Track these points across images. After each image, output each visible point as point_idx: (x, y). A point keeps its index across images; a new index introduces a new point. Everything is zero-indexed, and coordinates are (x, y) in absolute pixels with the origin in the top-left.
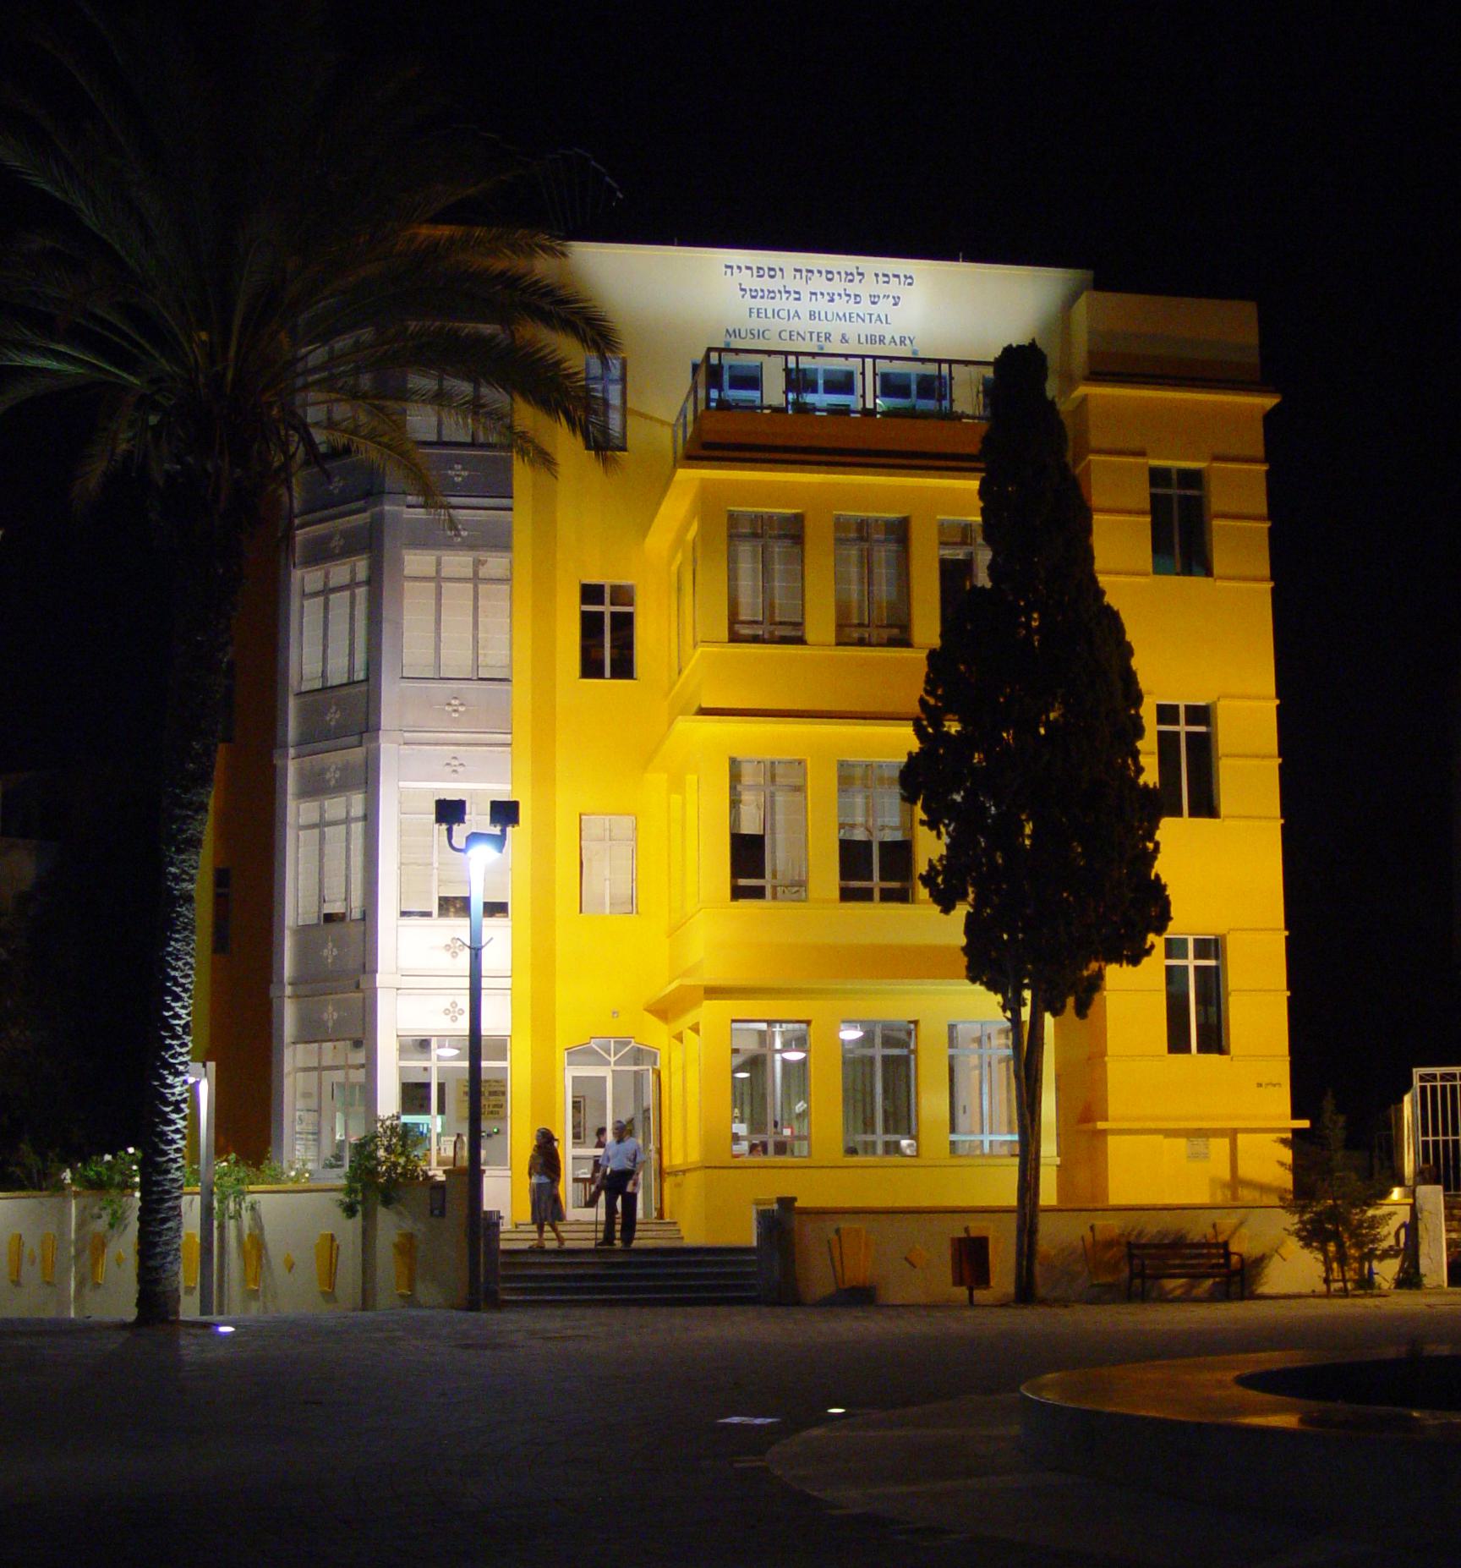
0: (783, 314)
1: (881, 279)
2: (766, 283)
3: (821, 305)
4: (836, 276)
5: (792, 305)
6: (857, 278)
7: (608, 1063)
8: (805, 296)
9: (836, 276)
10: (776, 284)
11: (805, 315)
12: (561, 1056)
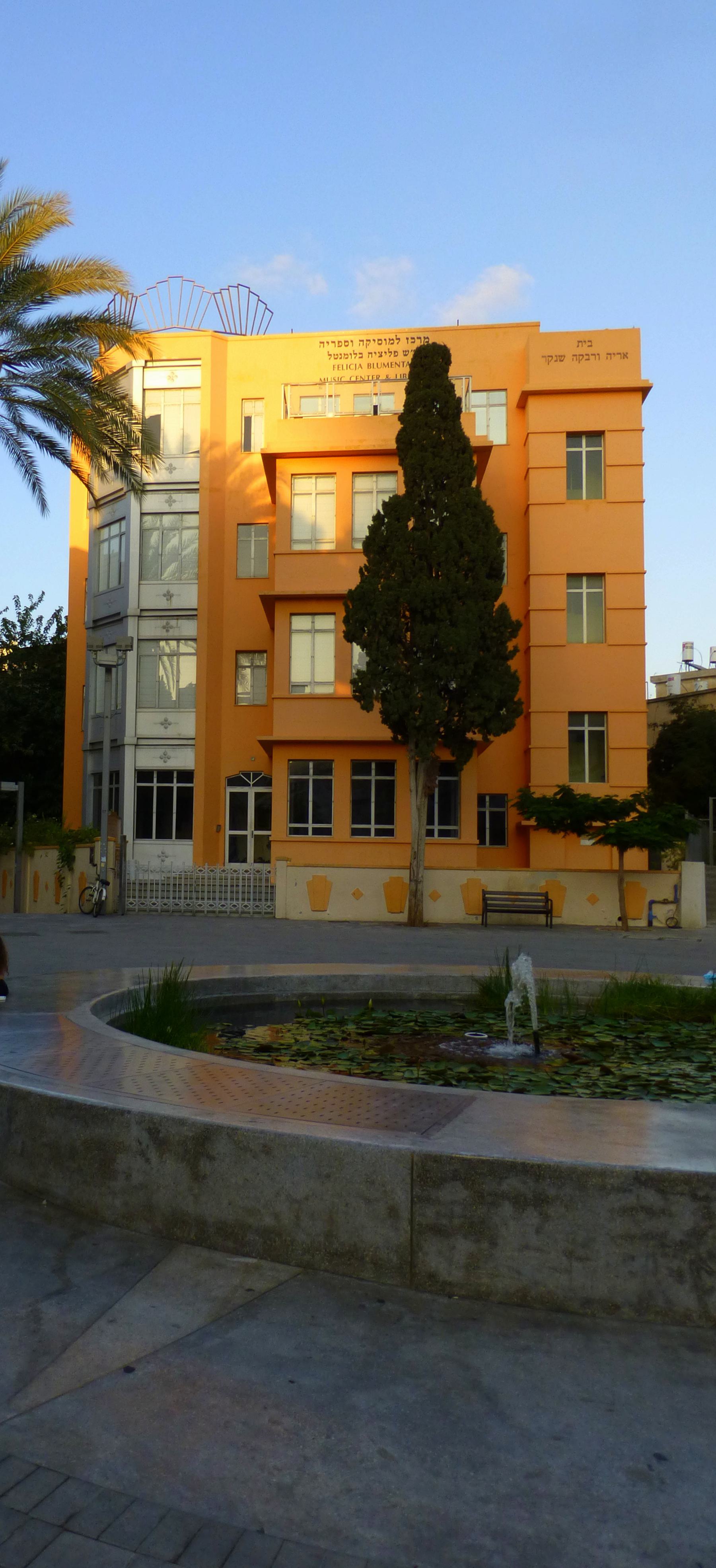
0: (353, 367)
1: (410, 340)
2: (343, 350)
3: (375, 359)
4: (384, 342)
5: (357, 361)
6: (396, 341)
7: (249, 785)
8: (365, 355)
9: (384, 342)
10: (348, 350)
11: (365, 366)
12: (224, 782)
